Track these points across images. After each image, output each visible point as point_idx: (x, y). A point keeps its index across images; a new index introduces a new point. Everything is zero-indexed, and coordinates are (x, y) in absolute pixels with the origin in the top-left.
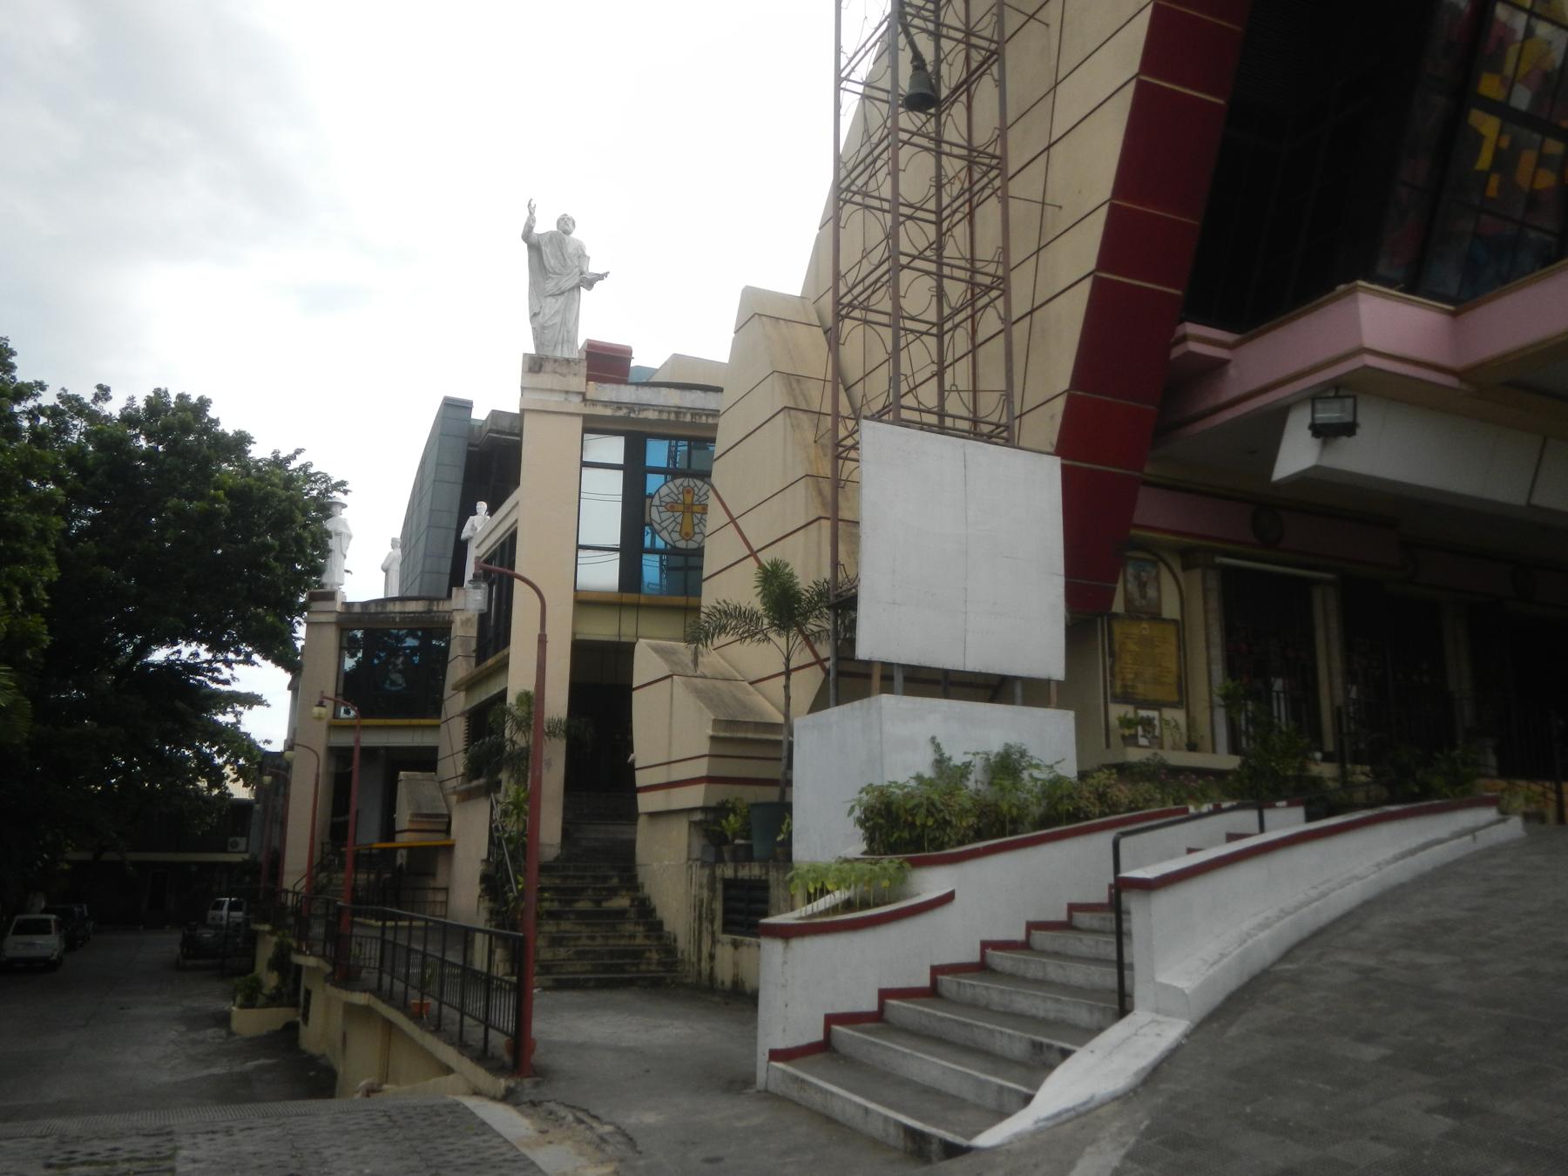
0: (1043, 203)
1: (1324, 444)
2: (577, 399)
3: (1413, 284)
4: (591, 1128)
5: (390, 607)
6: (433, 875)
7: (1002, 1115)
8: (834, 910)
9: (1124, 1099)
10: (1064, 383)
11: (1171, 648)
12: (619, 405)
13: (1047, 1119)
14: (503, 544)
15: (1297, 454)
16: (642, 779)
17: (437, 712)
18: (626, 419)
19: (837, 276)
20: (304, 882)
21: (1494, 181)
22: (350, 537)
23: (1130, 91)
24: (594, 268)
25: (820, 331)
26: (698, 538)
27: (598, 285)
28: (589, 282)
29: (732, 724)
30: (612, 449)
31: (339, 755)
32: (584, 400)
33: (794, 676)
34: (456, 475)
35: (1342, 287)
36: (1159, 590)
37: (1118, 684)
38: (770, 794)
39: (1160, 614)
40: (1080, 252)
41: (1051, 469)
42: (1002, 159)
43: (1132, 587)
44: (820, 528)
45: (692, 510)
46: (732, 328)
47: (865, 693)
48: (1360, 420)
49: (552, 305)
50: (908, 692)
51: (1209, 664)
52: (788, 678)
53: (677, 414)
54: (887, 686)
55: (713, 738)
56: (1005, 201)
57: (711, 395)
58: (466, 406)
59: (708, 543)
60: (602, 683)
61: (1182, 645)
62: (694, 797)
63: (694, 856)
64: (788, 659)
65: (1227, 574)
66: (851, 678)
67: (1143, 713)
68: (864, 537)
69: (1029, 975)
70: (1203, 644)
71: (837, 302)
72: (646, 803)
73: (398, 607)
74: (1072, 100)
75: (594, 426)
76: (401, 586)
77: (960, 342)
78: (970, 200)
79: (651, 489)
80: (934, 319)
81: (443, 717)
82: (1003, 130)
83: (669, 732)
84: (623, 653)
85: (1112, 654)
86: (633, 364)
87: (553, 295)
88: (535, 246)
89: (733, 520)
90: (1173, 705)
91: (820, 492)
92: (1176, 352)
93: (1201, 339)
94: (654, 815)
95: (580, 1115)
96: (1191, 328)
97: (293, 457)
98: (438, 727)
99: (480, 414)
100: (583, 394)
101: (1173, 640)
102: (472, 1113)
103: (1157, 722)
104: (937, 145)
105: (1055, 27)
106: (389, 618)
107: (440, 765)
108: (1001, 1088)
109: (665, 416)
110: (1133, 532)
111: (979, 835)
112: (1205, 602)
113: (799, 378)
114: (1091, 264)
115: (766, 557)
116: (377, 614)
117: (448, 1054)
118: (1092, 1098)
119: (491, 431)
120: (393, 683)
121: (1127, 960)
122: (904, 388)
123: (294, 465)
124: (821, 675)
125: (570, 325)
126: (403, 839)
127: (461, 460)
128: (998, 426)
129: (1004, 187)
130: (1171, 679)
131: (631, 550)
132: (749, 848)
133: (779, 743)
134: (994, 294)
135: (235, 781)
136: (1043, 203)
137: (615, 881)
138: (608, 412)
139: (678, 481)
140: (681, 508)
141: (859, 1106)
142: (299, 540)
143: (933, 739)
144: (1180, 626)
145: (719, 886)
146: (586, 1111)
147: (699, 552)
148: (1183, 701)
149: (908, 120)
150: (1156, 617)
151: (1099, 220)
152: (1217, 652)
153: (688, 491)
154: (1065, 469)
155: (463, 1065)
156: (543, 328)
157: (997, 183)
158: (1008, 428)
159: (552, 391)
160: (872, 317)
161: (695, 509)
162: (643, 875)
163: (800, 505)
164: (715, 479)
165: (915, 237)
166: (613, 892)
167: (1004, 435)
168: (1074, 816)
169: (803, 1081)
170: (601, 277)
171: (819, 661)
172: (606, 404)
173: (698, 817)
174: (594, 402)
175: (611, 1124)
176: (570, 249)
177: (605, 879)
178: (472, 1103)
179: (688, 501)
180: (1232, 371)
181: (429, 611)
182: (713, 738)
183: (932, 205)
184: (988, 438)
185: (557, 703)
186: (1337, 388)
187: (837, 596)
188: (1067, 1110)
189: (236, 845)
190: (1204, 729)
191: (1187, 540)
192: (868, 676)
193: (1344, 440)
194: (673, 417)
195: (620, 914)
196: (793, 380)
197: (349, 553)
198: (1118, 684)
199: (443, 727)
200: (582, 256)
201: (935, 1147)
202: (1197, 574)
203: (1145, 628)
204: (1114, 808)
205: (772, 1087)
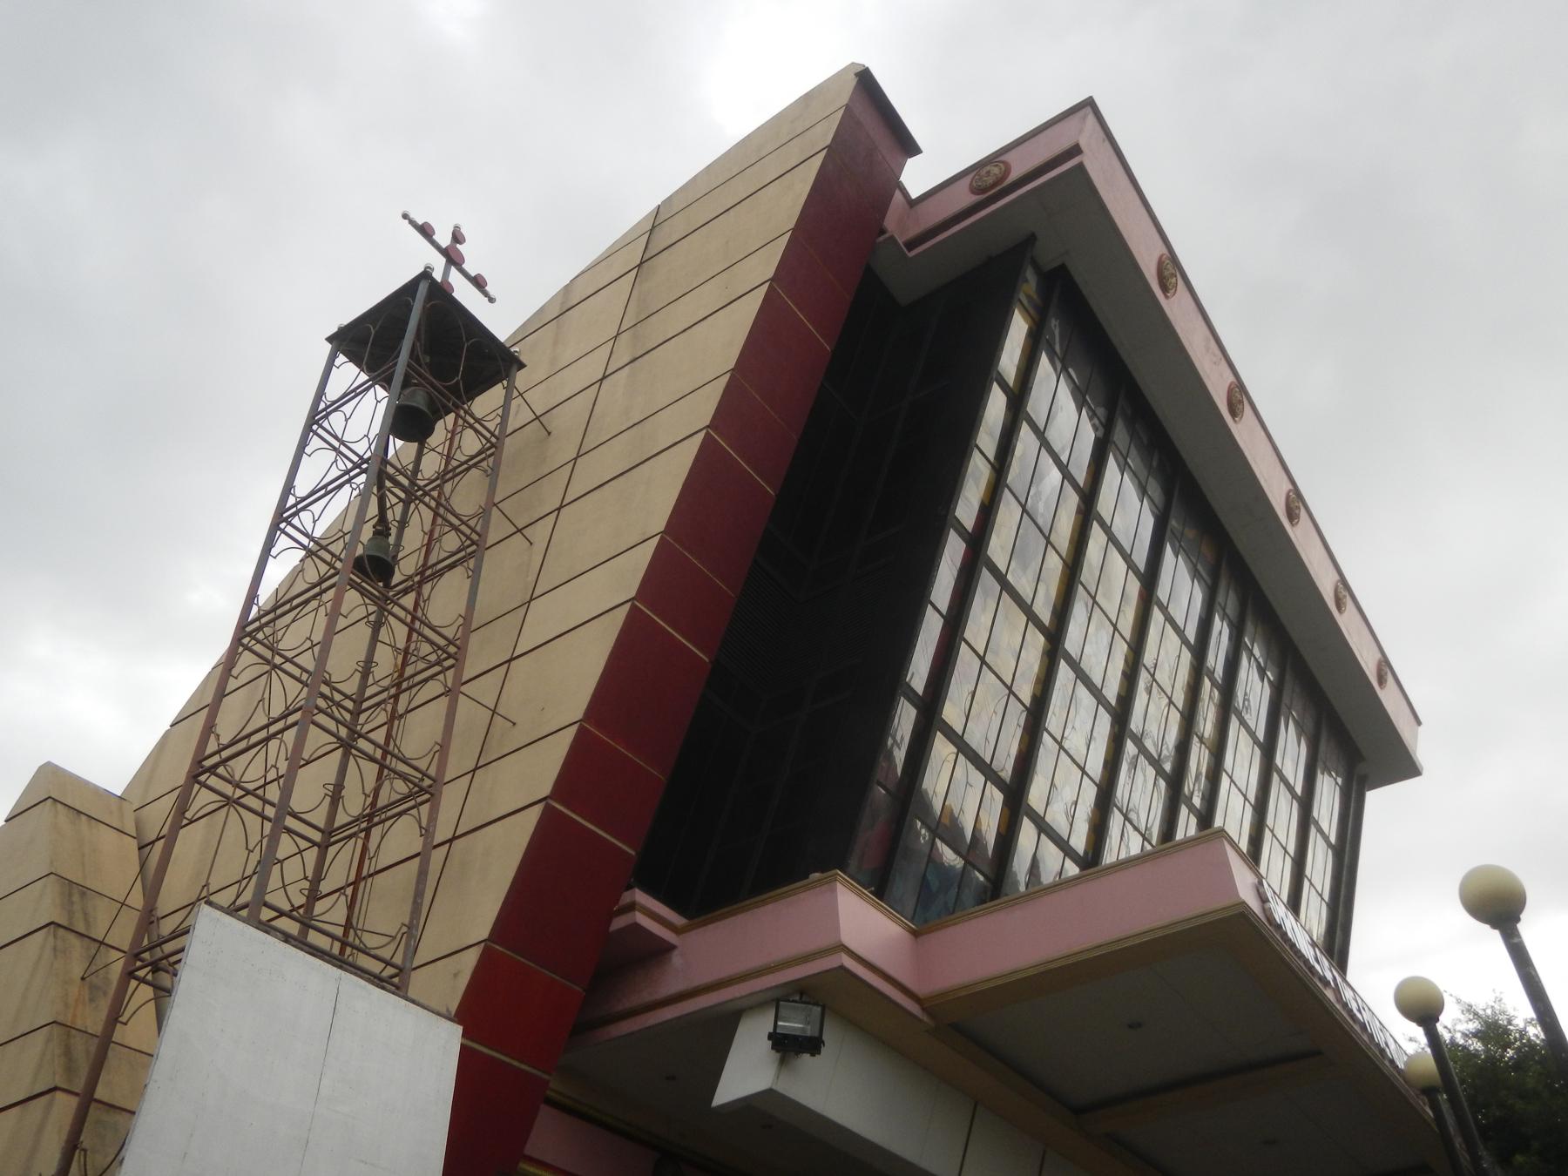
0: (494, 712)
1: (783, 1062)
10: (482, 930)
15: (747, 1072)
23: (621, 615)
25: (134, 844)
35: (817, 875)
41: (450, 1038)
44: (50, 1105)
46: (5, 817)
48: (824, 1038)
71: (198, 761)
74: (545, 618)
77: (339, 870)
91: (67, 1052)
92: (618, 923)
93: (648, 912)
96: (640, 897)
105: (540, 546)
113: (85, 891)
114: (546, 789)
136: (494, 712)
151: (560, 747)
158: (401, 970)
167: (394, 981)
180: (676, 959)
186: (802, 994)
193: (806, 1056)
196: (74, 891)
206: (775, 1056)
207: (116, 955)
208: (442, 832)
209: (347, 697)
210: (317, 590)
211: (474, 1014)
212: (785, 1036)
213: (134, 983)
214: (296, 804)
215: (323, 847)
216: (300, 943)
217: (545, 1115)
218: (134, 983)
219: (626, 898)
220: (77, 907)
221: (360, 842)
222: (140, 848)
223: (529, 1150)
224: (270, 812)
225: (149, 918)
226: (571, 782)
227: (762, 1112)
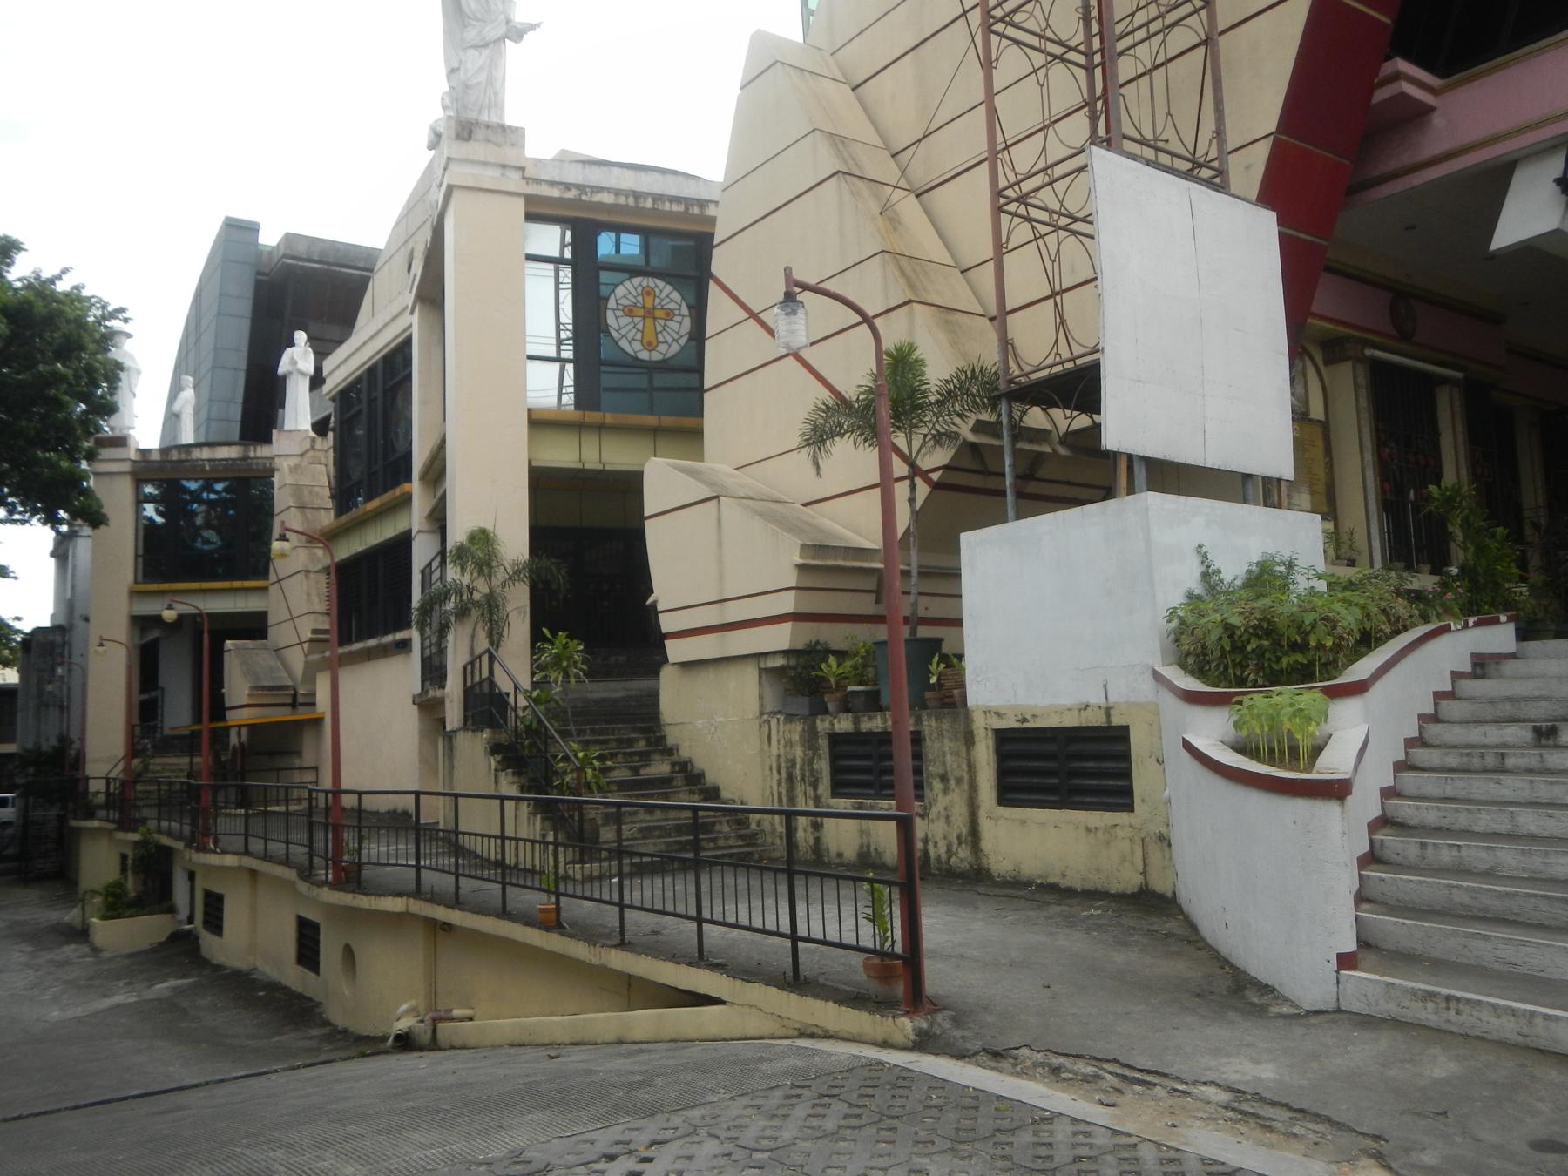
5: (197, 454)
6: (299, 753)
10: (1272, 126)
14: (371, 371)
16: (667, 623)
20: (121, 767)
22: (139, 372)
24: (520, 16)
28: (517, 33)
29: (821, 549)
31: (142, 623)
34: (244, 307)
46: (738, 84)
47: (1108, 493)
49: (475, 60)
55: (802, 568)
62: (780, 638)
63: (768, 709)
69: (1457, 826)
72: (677, 650)
73: (206, 454)
76: (197, 430)
87: (476, 47)
91: (903, 272)
94: (687, 666)
97: (59, 278)
98: (265, 589)
99: (269, 237)
100: (523, 169)
101: (1320, 444)
106: (195, 470)
107: (271, 632)
109: (622, 200)
112: (1357, 400)
119: (285, 256)
120: (206, 541)
126: (233, 717)
127: (248, 291)
137: (641, 745)
138: (555, 193)
139: (637, 281)
140: (641, 312)
142: (90, 370)
143: (1200, 546)
145: (823, 743)
146: (1116, 1061)
153: (648, 292)
156: (466, 86)
159: (485, 164)
161: (658, 314)
162: (672, 736)
166: (645, 757)
170: (532, 27)
173: (779, 662)
174: (538, 181)
177: (631, 742)
180: (1437, 120)
181: (245, 458)
185: (515, 543)
191: (1340, 329)
194: (631, 201)
195: (665, 782)
196: (838, 141)
199: (274, 590)
219: (1387, 68)
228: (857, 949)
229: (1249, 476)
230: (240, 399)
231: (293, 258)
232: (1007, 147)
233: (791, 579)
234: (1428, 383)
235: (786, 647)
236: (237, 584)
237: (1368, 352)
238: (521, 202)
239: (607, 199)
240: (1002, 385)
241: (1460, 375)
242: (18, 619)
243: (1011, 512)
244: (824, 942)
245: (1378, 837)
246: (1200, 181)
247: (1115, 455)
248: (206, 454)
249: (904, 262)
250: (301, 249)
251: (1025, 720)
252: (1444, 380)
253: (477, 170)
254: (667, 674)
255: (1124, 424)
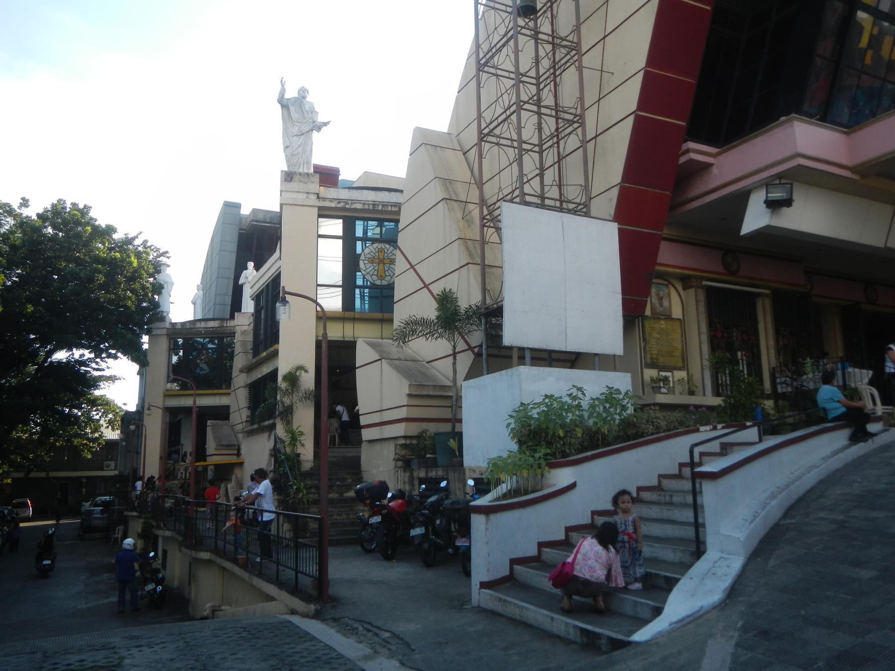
0: (602, 71)
2: (314, 197)
3: (824, 115)
4: (377, 635)
5: (198, 325)
7: (645, 622)
8: (505, 496)
9: (721, 606)
11: (678, 335)
12: (339, 201)
13: (677, 622)
14: (267, 286)
15: (755, 218)
16: (363, 421)
17: (229, 387)
18: (343, 209)
19: (480, 116)
21: (870, 53)
22: (173, 284)
24: (321, 119)
26: (388, 278)
27: (324, 129)
28: (319, 128)
29: (420, 386)
30: (335, 227)
32: (318, 198)
33: (458, 356)
34: (233, 246)
35: (783, 118)
36: (670, 301)
37: (649, 357)
38: (446, 428)
39: (670, 315)
40: (627, 98)
41: (612, 229)
42: (579, 44)
43: (655, 300)
44: (468, 270)
45: (384, 262)
46: (408, 153)
47: (509, 366)
48: (794, 197)
50: (532, 365)
51: (700, 343)
52: (455, 359)
53: (374, 205)
54: (522, 360)
55: (410, 395)
56: (580, 69)
57: (393, 194)
58: (238, 206)
59: (397, 281)
60: (337, 365)
61: (684, 333)
62: (399, 430)
64: (454, 347)
65: (709, 291)
66: (496, 355)
67: (663, 374)
68: (505, 272)
70: (696, 331)
71: (480, 132)
72: (366, 434)
73: (203, 325)
75: (325, 213)
77: (550, 157)
78: (554, 73)
79: (359, 250)
80: (536, 142)
81: (232, 389)
82: (577, 29)
83: (380, 391)
84: (347, 348)
85: (644, 340)
86: (340, 178)
88: (284, 104)
89: (412, 267)
90: (680, 369)
91: (467, 248)
92: (683, 160)
93: (697, 151)
94: (371, 441)
95: (365, 625)
97: (137, 237)
99: (245, 211)
101: (679, 331)
102: (298, 627)
103: (671, 379)
104: (535, 35)
106: (199, 334)
107: (231, 416)
108: (636, 602)
109: (366, 207)
110: (658, 268)
111: (584, 449)
112: (697, 309)
113: (451, 181)
114: (634, 107)
115: (437, 289)
116: (191, 329)
117: (271, 589)
118: (702, 608)
120: (202, 369)
121: (700, 521)
122: (525, 180)
123: (136, 242)
124: (472, 357)
125: (308, 153)
126: (212, 460)
128: (580, 204)
129: (580, 60)
130: (678, 353)
131: (348, 286)
132: (435, 459)
133: (451, 397)
134: (576, 125)
135: (107, 427)
137: (350, 480)
138: (333, 205)
139: (375, 245)
141: (547, 616)
144: (682, 322)
146: (370, 623)
147: (391, 287)
148: (684, 367)
149: (521, 22)
150: (668, 317)
152: (705, 338)
154: (619, 229)
155: (284, 596)
157: (576, 58)
160: (502, 141)
161: (386, 261)
163: (455, 256)
164: (400, 243)
165: (528, 92)
167: (583, 210)
168: (636, 436)
169: (505, 601)
170: (326, 124)
171: (471, 348)
172: (331, 200)
173: (403, 441)
174: (324, 199)
175: (388, 631)
176: (307, 107)
178: (295, 620)
179: (381, 257)
180: (715, 170)
181: (222, 327)
182: (410, 396)
183: (533, 73)
184: (574, 212)
187: (486, 308)
188: (688, 616)
189: (108, 466)
190: (698, 382)
191: (686, 272)
192: (511, 357)
193: (785, 209)
194: (371, 207)
197: (172, 294)
198: (649, 357)
199: (233, 394)
200: (313, 111)
201: (604, 641)
202: (692, 291)
203: (663, 324)
204: (658, 429)
205: (482, 605)
206: (769, 210)
207: (471, 207)
208: (590, 135)
209: (535, 145)
210: (505, 39)
211: (622, 215)
212: (773, 201)
213: (486, 229)
214: (524, 138)
215: (541, 153)
216: (542, 206)
217: (664, 245)
218: (486, 229)
219: (685, 146)
220: (450, 189)
221: (556, 149)
222: (464, 154)
223: (658, 261)
224: (516, 144)
225: (483, 202)
226: (647, 99)
227: (764, 234)
228: (309, 576)
229: (595, 355)
230: (230, 293)
231: (257, 221)
232: (528, 181)
233: (405, 401)
234: (752, 297)
235: (402, 434)
236: (216, 391)
237: (704, 283)
238: (316, 209)
239: (359, 206)
240: (482, 310)
241: (767, 291)
242: (125, 404)
243: (485, 372)
244: (305, 574)
245: (570, 534)
246: (569, 211)
247: (511, 348)
248: (203, 325)
249: (470, 243)
250: (261, 217)
251: (482, 474)
252: (759, 295)
253: (295, 195)
254: (364, 446)
255: (514, 333)
